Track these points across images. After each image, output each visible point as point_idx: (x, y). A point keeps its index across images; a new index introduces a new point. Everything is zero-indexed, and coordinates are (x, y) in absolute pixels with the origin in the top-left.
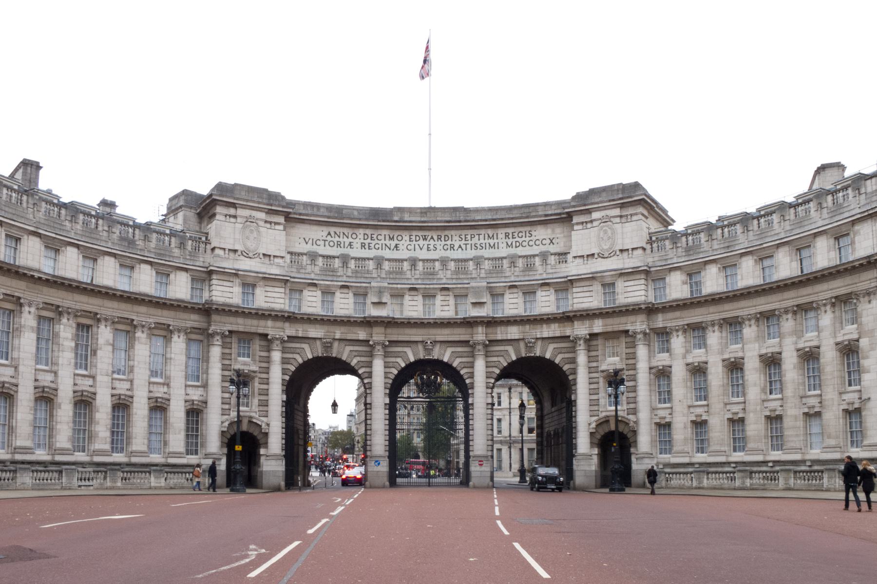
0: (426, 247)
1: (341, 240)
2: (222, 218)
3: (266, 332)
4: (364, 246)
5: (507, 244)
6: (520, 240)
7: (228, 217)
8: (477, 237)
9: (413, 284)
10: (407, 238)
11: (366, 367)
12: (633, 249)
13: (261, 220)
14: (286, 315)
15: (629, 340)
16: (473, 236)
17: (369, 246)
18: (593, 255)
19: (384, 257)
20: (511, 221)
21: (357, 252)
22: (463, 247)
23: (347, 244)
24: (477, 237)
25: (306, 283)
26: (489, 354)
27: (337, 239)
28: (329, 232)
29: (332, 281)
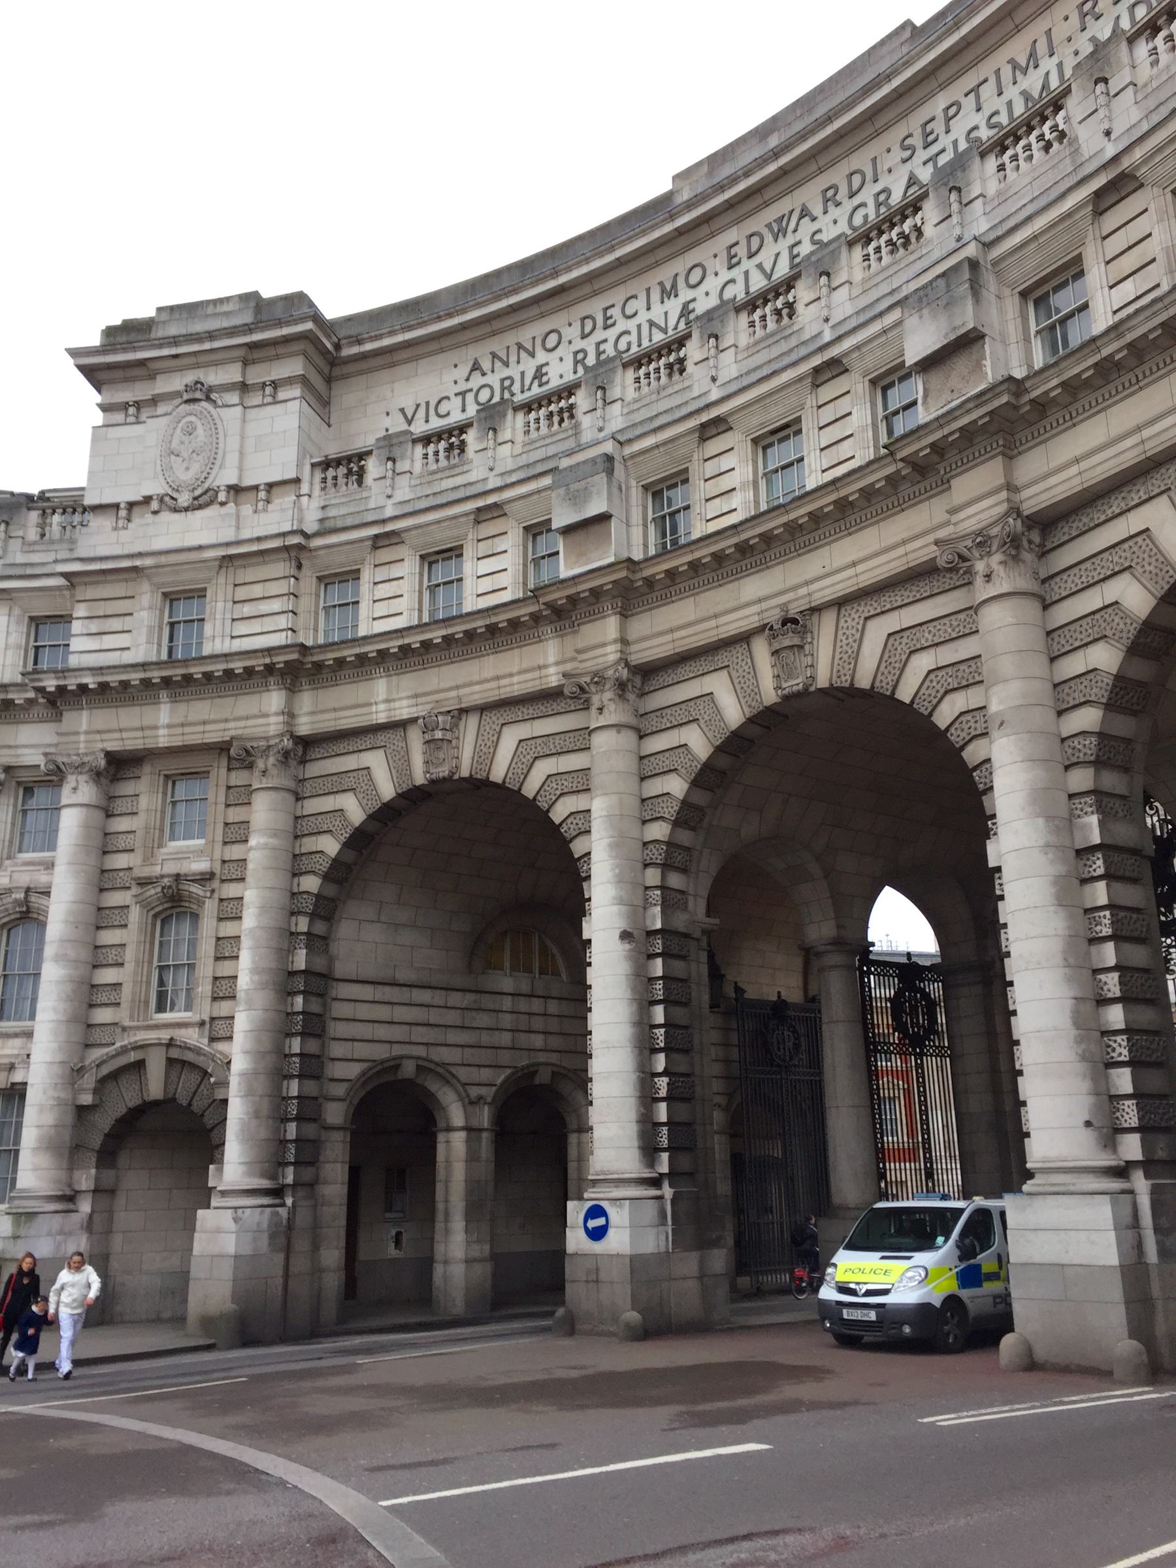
7: (132, 410)
8: (969, 103)
14: (280, 659)
16: (952, 111)
23: (527, 382)
24: (969, 103)
25: (361, 540)
26: (1060, 587)
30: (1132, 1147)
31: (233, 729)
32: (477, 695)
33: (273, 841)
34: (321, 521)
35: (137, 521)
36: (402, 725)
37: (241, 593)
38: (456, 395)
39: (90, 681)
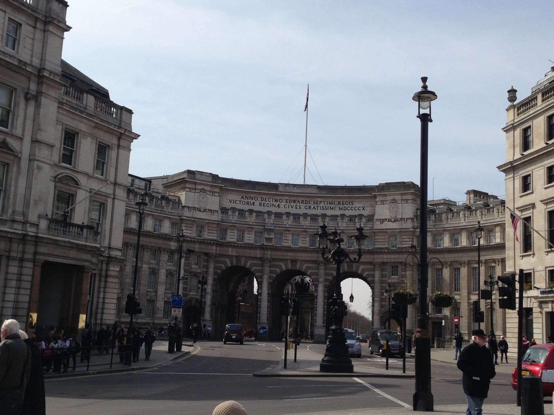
0: (295, 206)
2: (189, 190)
3: (207, 252)
4: (261, 205)
5: (340, 208)
6: (347, 206)
8: (323, 202)
11: (259, 272)
12: (407, 218)
13: (208, 191)
14: (219, 243)
15: (403, 267)
17: (264, 205)
18: (386, 219)
19: (272, 212)
20: (343, 196)
21: (257, 208)
22: (316, 208)
23: (251, 204)
28: (243, 196)
30: (325, 324)
31: (208, 251)
32: (246, 255)
33: (212, 270)
34: (222, 219)
35: (192, 211)
36: (232, 256)
37: (209, 228)
39: (189, 239)
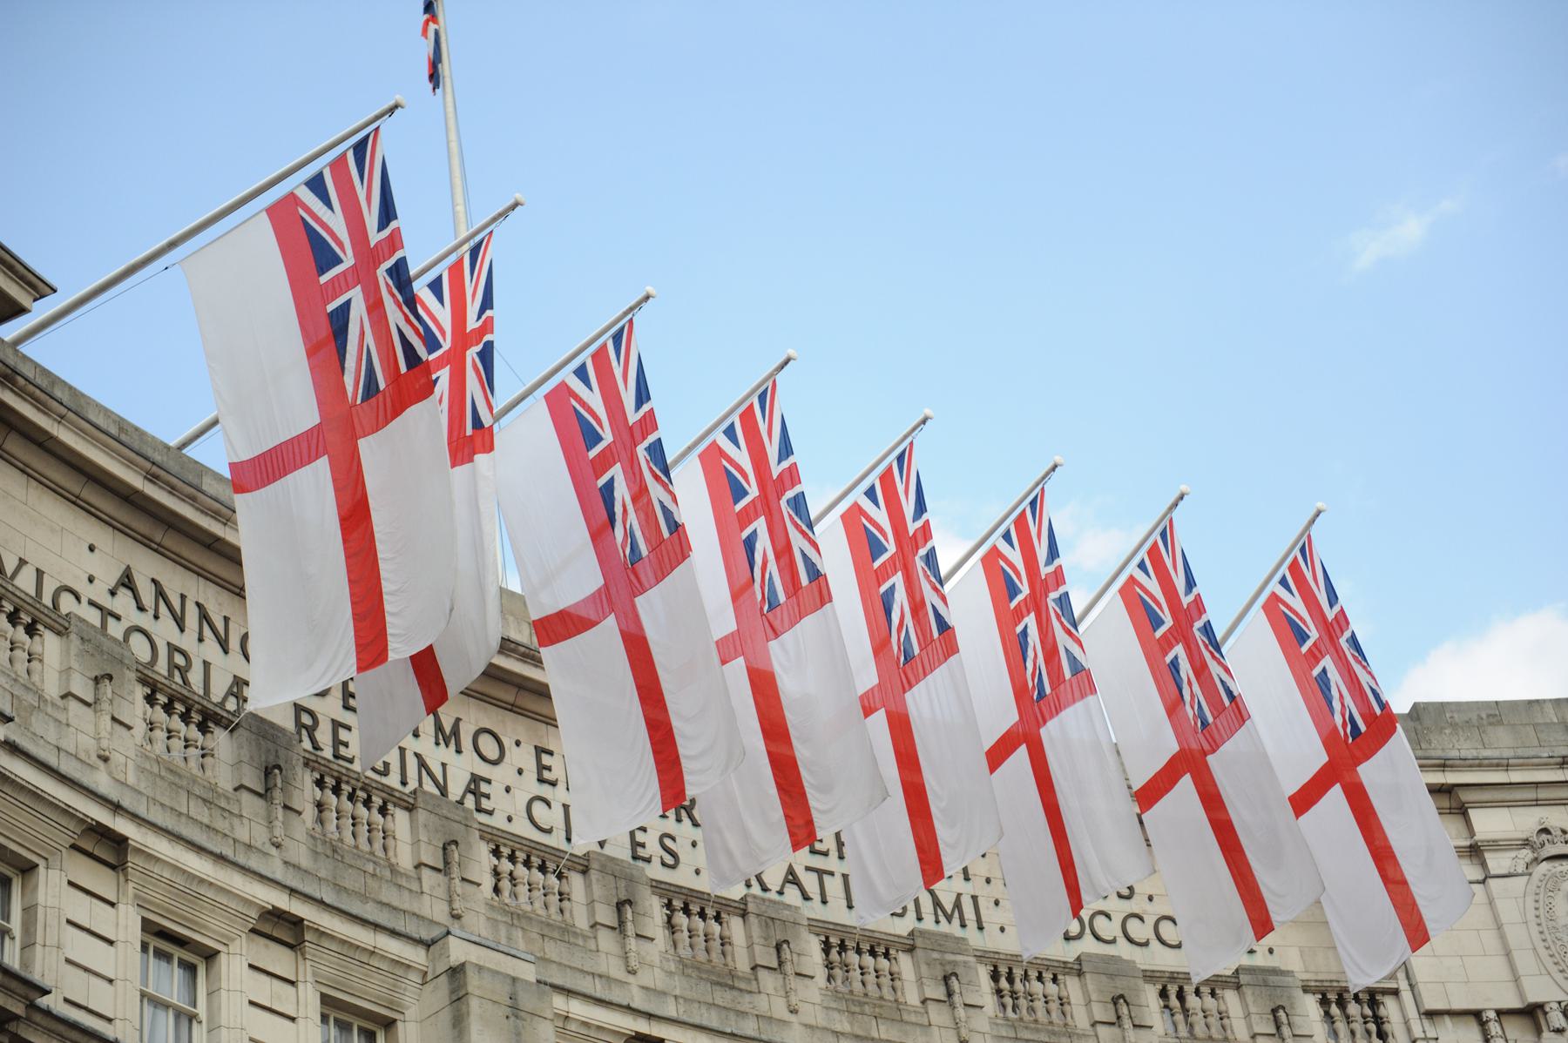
1: (187, 641)
9: (650, 1016)
10: (522, 757)
25: (67, 812)
27: (165, 630)
29: (220, 858)
38: (92, 603)
